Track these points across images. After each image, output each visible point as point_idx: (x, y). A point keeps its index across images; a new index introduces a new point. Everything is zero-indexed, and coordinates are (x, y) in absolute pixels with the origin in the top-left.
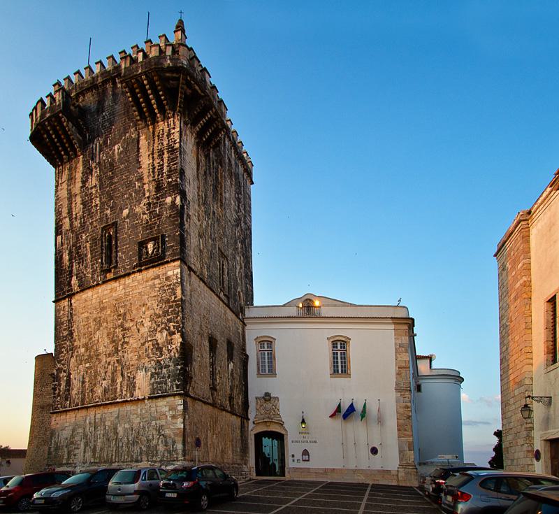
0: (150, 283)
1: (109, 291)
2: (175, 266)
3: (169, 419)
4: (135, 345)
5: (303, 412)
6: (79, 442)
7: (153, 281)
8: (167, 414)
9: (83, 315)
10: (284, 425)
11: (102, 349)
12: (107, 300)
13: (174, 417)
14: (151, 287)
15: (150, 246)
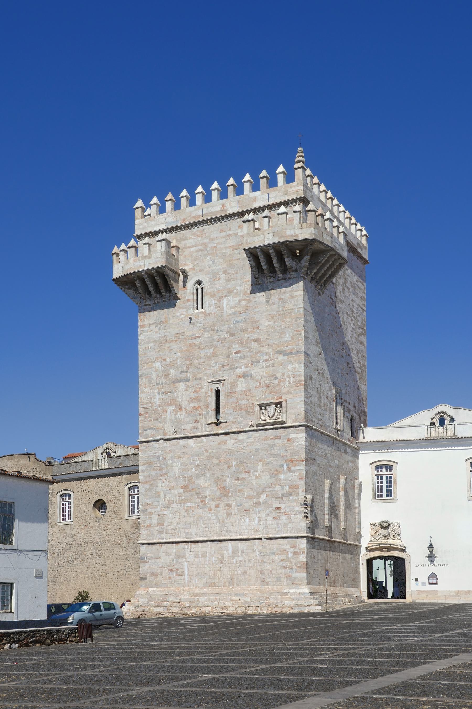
0: (271, 442)
1: (217, 443)
2: (298, 430)
3: (290, 555)
4: (250, 493)
5: (431, 537)
6: (180, 570)
7: (272, 440)
8: (288, 550)
9: (181, 460)
10: (407, 550)
11: (208, 493)
12: (214, 451)
13: (295, 553)
14: (270, 446)
15: (271, 409)
